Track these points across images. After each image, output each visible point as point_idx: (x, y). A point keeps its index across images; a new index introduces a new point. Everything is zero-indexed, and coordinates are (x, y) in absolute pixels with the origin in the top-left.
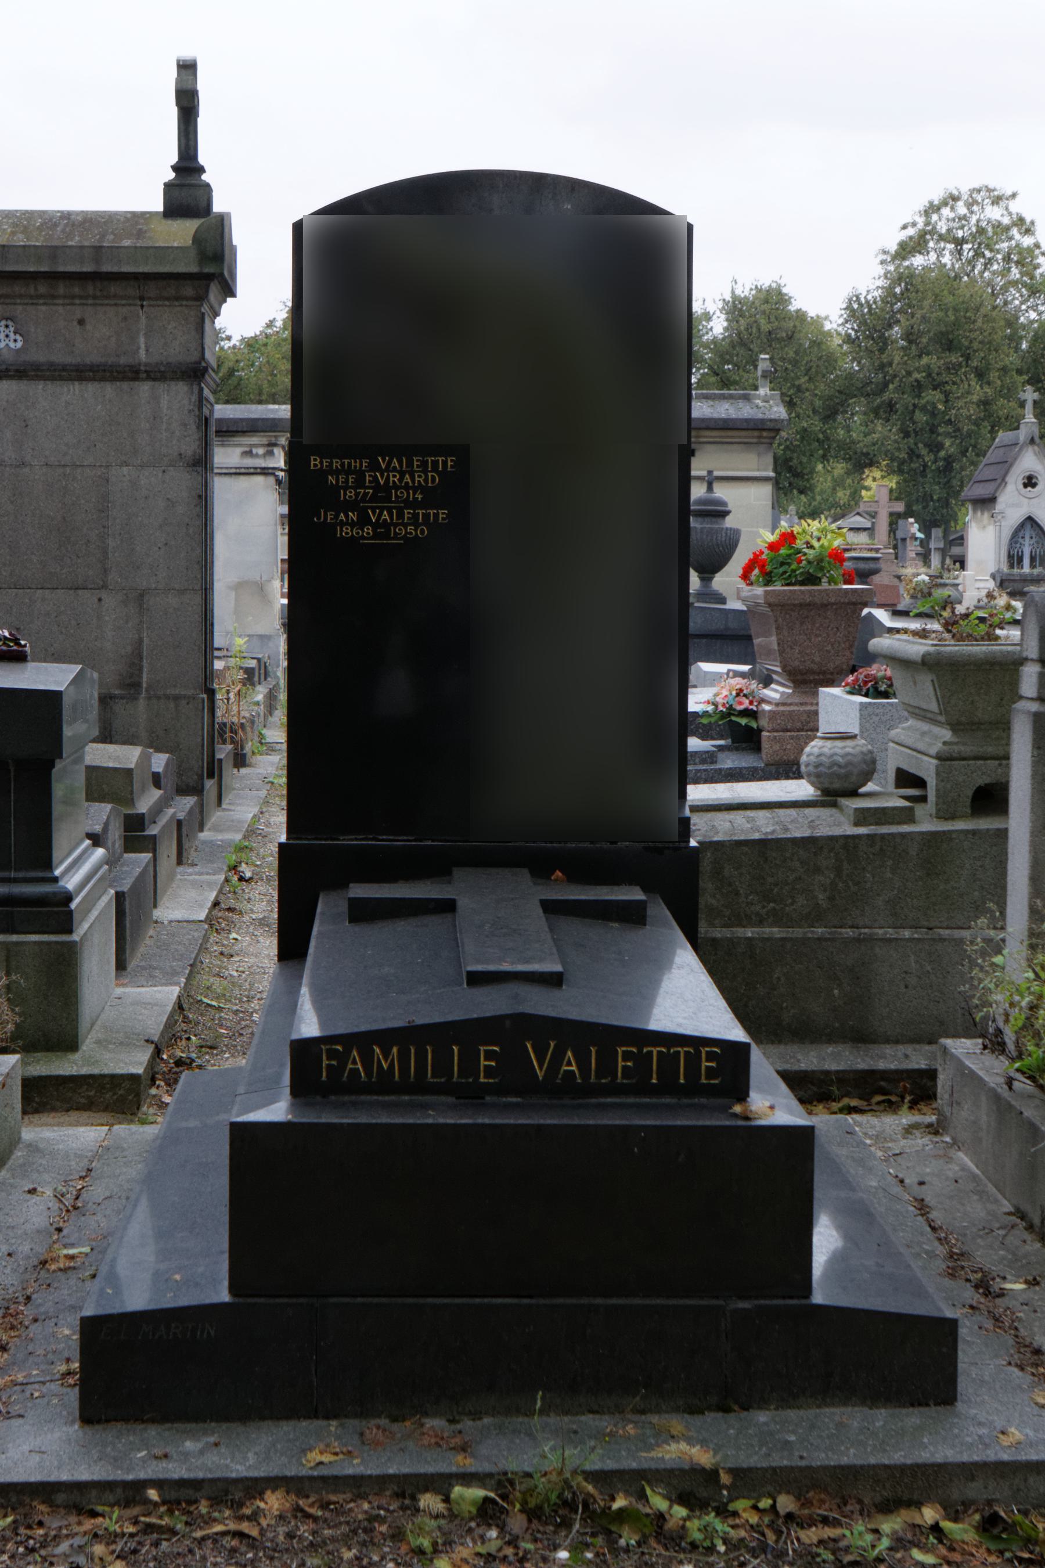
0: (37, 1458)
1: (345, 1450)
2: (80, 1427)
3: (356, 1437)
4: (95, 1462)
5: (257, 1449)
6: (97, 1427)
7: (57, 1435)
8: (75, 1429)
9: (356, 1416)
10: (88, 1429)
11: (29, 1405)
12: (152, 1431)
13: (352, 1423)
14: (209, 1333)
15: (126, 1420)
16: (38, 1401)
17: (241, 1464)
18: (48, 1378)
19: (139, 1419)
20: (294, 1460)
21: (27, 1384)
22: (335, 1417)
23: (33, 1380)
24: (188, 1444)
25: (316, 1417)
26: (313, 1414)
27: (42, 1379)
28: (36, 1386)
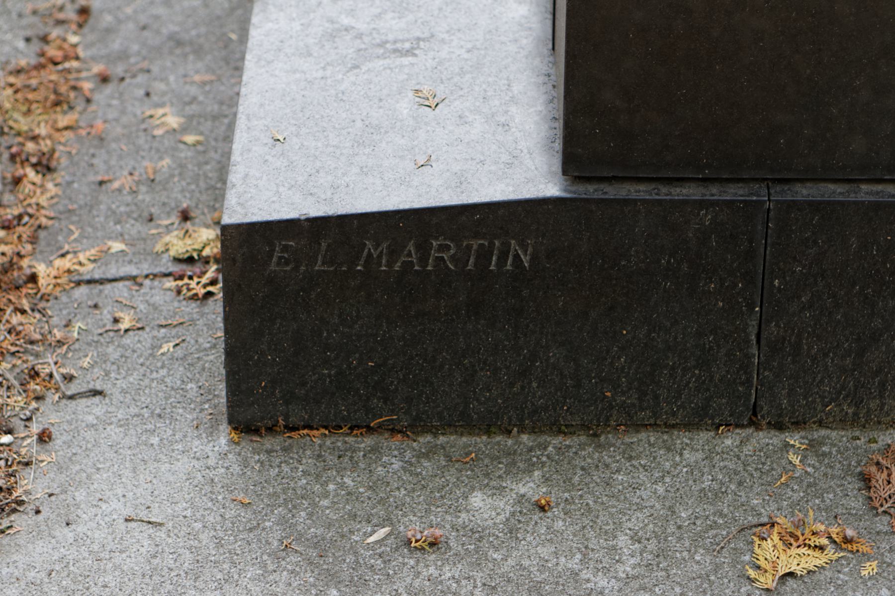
0: (141, 535)
1: (834, 530)
2: (232, 442)
3: (853, 485)
4: (274, 555)
5: (635, 521)
6: (269, 442)
7: (184, 465)
8: (224, 437)
9: (843, 422)
10: (247, 446)
11: (113, 352)
12: (394, 458)
13: (835, 438)
14: (517, 257)
15: (333, 426)
16: (128, 340)
17: (606, 570)
18: (146, 268)
19: (362, 427)
20: (725, 558)
21: (101, 282)
22: (798, 424)
23: (112, 272)
24: (477, 500)
25: (754, 424)
26: (752, 418)
27: (132, 270)
28: (121, 290)
